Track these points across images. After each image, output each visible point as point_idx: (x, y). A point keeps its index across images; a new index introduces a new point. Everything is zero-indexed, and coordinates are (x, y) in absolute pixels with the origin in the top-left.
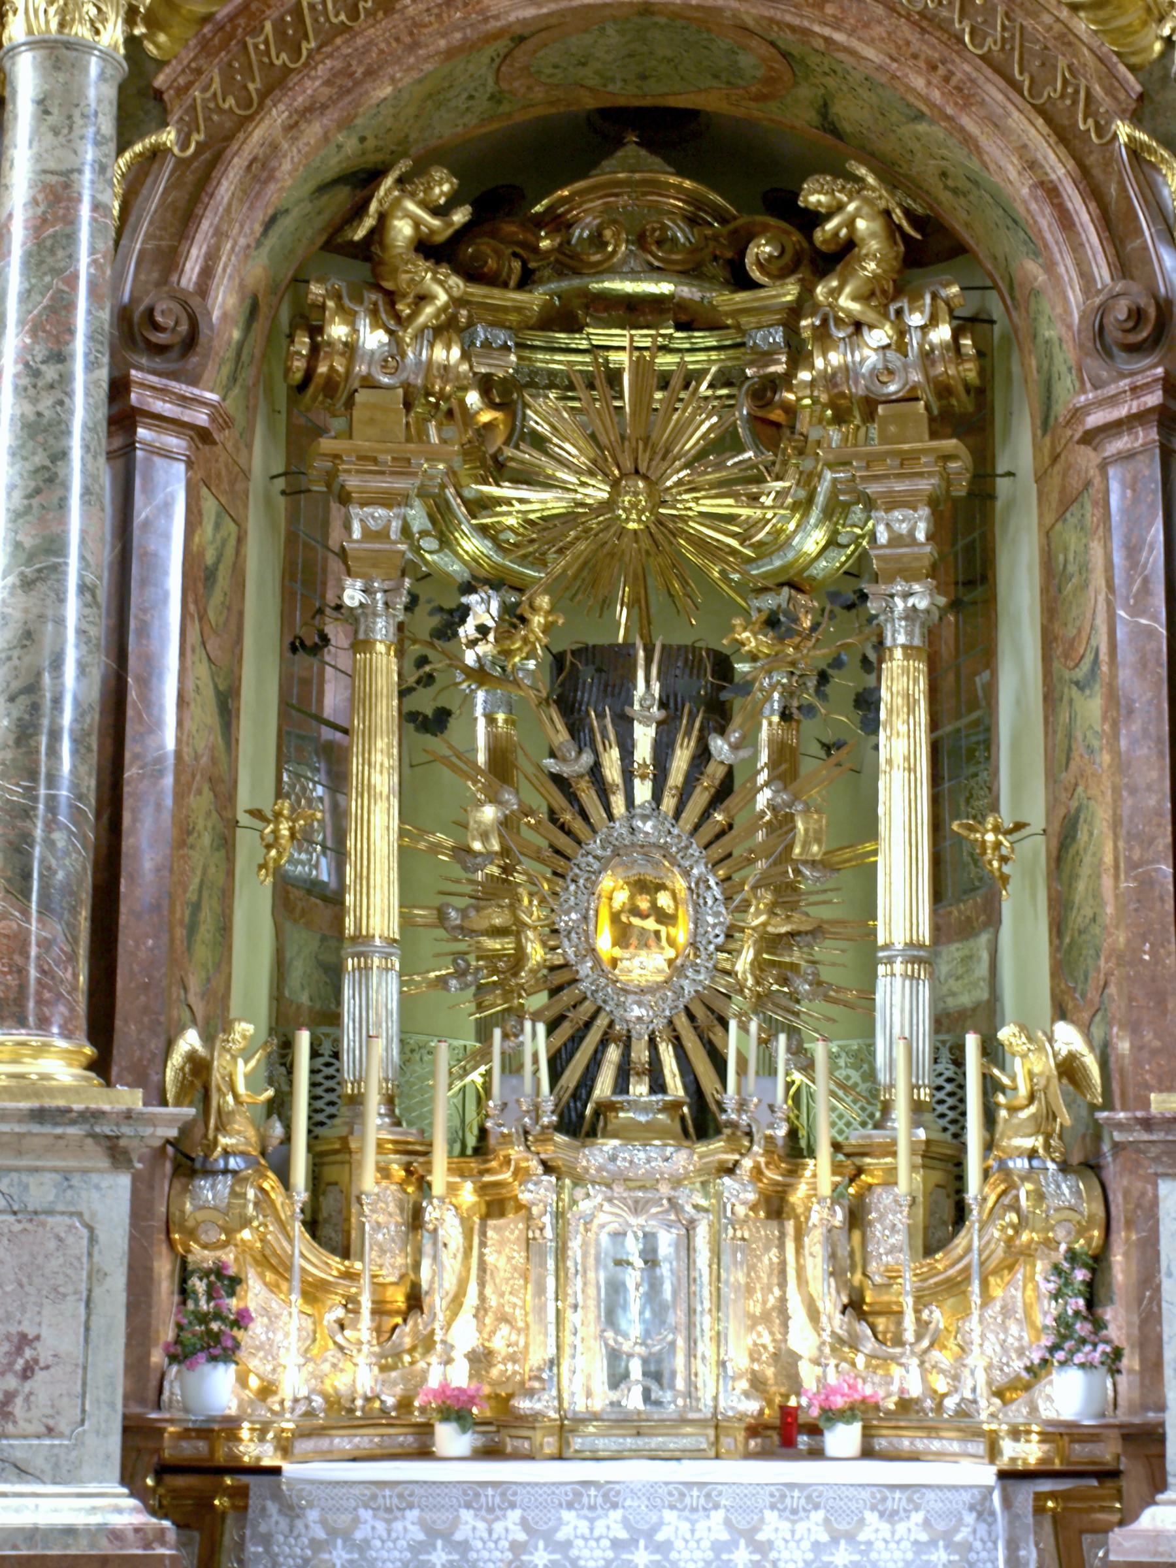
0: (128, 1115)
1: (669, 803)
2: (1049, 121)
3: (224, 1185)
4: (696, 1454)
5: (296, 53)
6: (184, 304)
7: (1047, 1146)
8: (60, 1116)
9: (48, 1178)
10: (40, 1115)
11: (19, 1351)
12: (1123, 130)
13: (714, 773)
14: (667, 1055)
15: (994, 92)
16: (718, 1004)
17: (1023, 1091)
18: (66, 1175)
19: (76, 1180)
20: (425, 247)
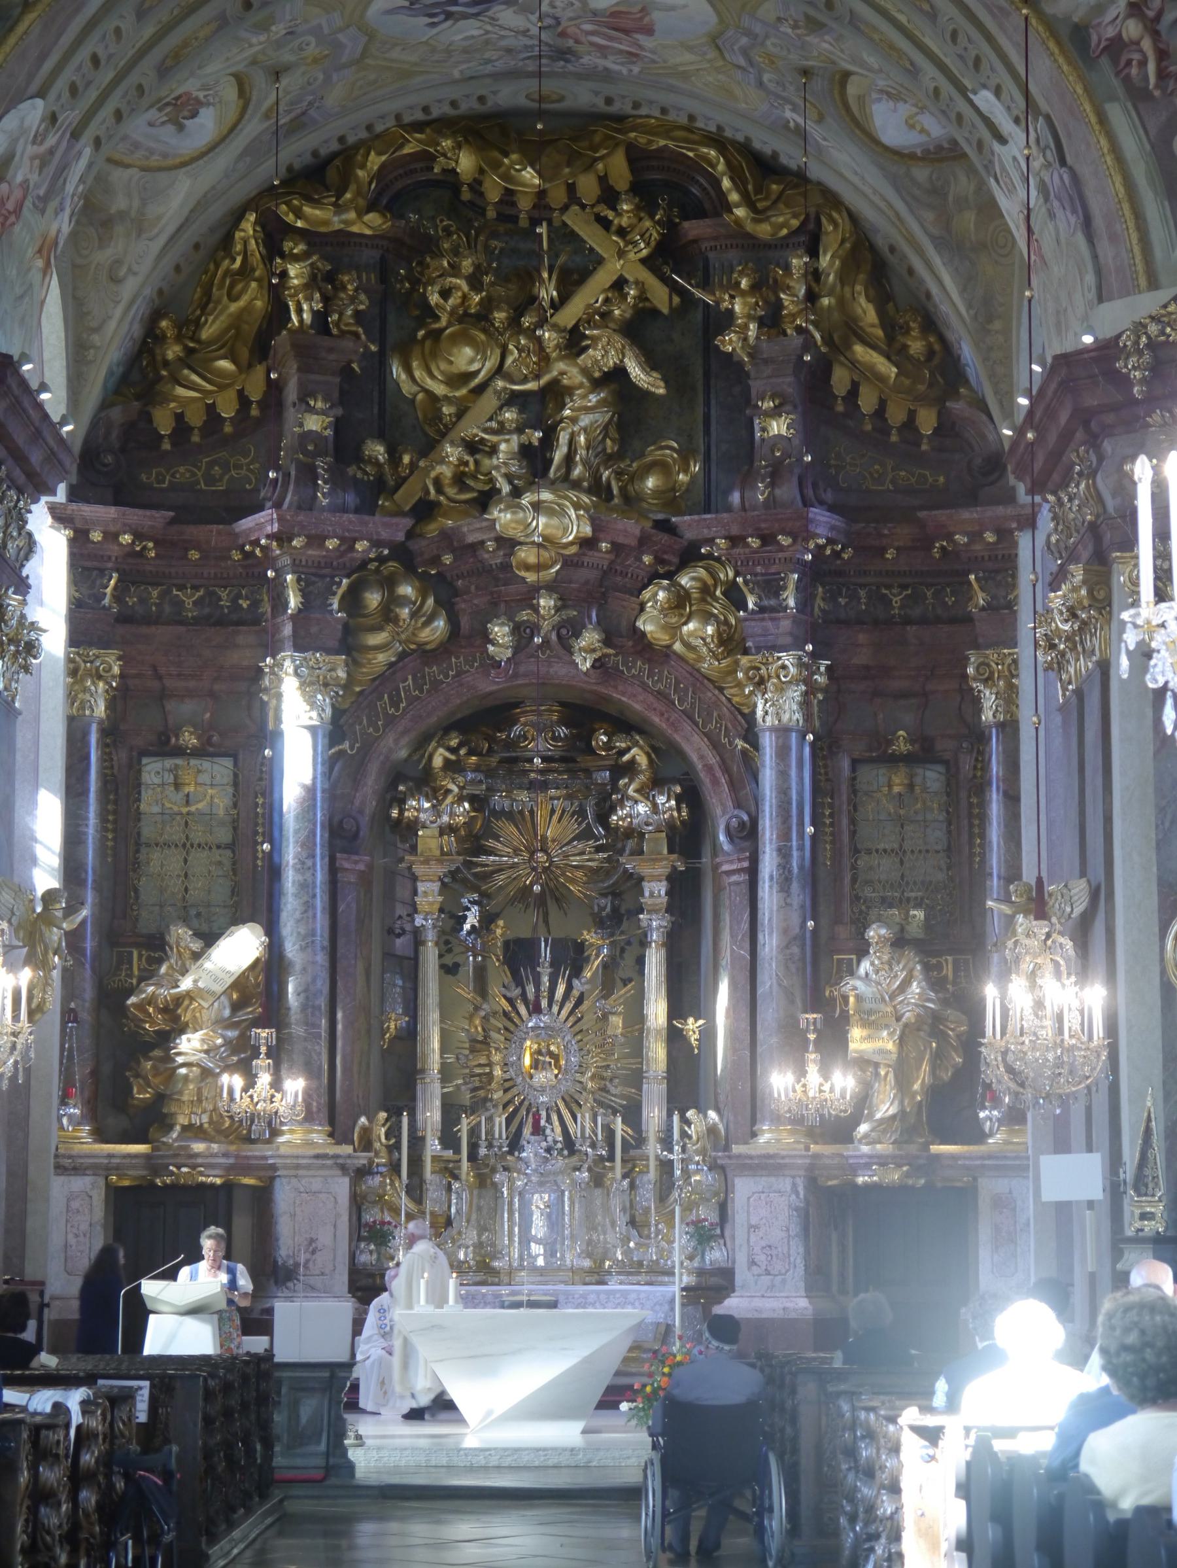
0: (349, 1156)
1: (555, 1009)
2: (709, 739)
3: (378, 1179)
4: (566, 1283)
5: (397, 710)
6: (354, 819)
7: (704, 1160)
8: (325, 1156)
9: (319, 1179)
10: (317, 1157)
11: (310, 1244)
12: (740, 744)
13: (576, 993)
14: (555, 1118)
15: (687, 727)
16: (577, 1096)
17: (694, 1137)
18: (325, 1177)
19: (329, 1180)
20: (448, 765)
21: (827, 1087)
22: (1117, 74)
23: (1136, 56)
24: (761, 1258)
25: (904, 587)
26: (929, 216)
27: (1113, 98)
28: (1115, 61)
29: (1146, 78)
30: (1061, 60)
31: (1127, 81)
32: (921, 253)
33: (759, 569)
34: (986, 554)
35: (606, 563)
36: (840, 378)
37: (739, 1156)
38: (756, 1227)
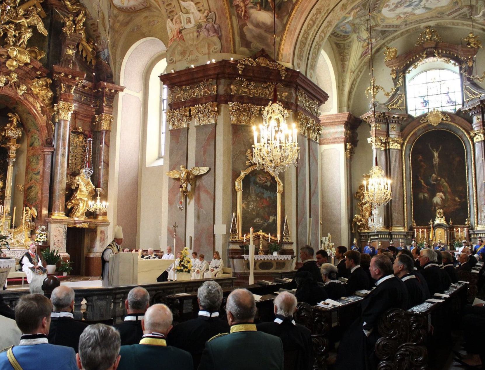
12: (50, 122)
21: (102, 205)
22: (236, 11)
23: (241, 10)
24: (56, 243)
25: (85, 96)
26: (111, 21)
27: (234, 15)
28: (237, 8)
29: (242, 14)
30: (225, 3)
31: (238, 13)
32: (105, 27)
33: (67, 83)
34: (109, 94)
35: (27, 71)
36: (80, 47)
37: (55, 219)
38: (56, 236)
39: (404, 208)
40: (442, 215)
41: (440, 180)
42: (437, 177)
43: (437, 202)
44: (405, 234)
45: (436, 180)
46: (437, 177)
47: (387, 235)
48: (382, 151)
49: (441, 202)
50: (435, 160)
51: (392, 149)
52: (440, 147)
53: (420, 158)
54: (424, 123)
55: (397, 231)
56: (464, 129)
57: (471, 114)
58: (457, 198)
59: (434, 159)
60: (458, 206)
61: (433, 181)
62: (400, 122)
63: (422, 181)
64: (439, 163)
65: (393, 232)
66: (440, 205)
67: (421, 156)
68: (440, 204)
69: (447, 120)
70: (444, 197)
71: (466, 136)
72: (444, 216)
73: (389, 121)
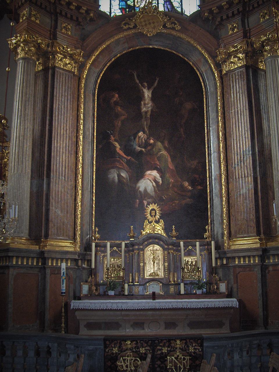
39: (75, 200)
40: (158, 217)
41: (153, 145)
42: (149, 138)
43: (145, 190)
44: (76, 257)
45: (146, 144)
46: (149, 138)
47: (33, 258)
48: (38, 72)
49: (155, 191)
50: (145, 104)
51: (60, 68)
52: (156, 80)
53: (115, 99)
54: (129, 29)
55: (57, 249)
56: (204, 48)
57: (219, 19)
58: (186, 184)
59: (142, 103)
60: (188, 200)
61: (139, 146)
62: (80, 20)
63: (117, 145)
64: (152, 110)
65: (49, 251)
66: (151, 197)
67: (117, 95)
68: (153, 194)
69: (173, 29)
70: (160, 180)
71: (207, 61)
72: (161, 217)
73: (58, 11)
